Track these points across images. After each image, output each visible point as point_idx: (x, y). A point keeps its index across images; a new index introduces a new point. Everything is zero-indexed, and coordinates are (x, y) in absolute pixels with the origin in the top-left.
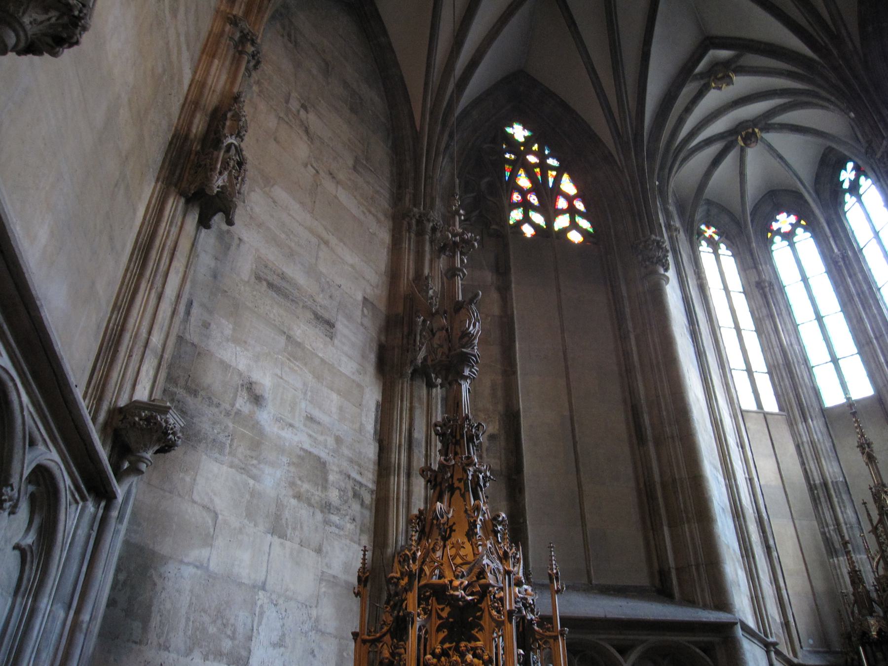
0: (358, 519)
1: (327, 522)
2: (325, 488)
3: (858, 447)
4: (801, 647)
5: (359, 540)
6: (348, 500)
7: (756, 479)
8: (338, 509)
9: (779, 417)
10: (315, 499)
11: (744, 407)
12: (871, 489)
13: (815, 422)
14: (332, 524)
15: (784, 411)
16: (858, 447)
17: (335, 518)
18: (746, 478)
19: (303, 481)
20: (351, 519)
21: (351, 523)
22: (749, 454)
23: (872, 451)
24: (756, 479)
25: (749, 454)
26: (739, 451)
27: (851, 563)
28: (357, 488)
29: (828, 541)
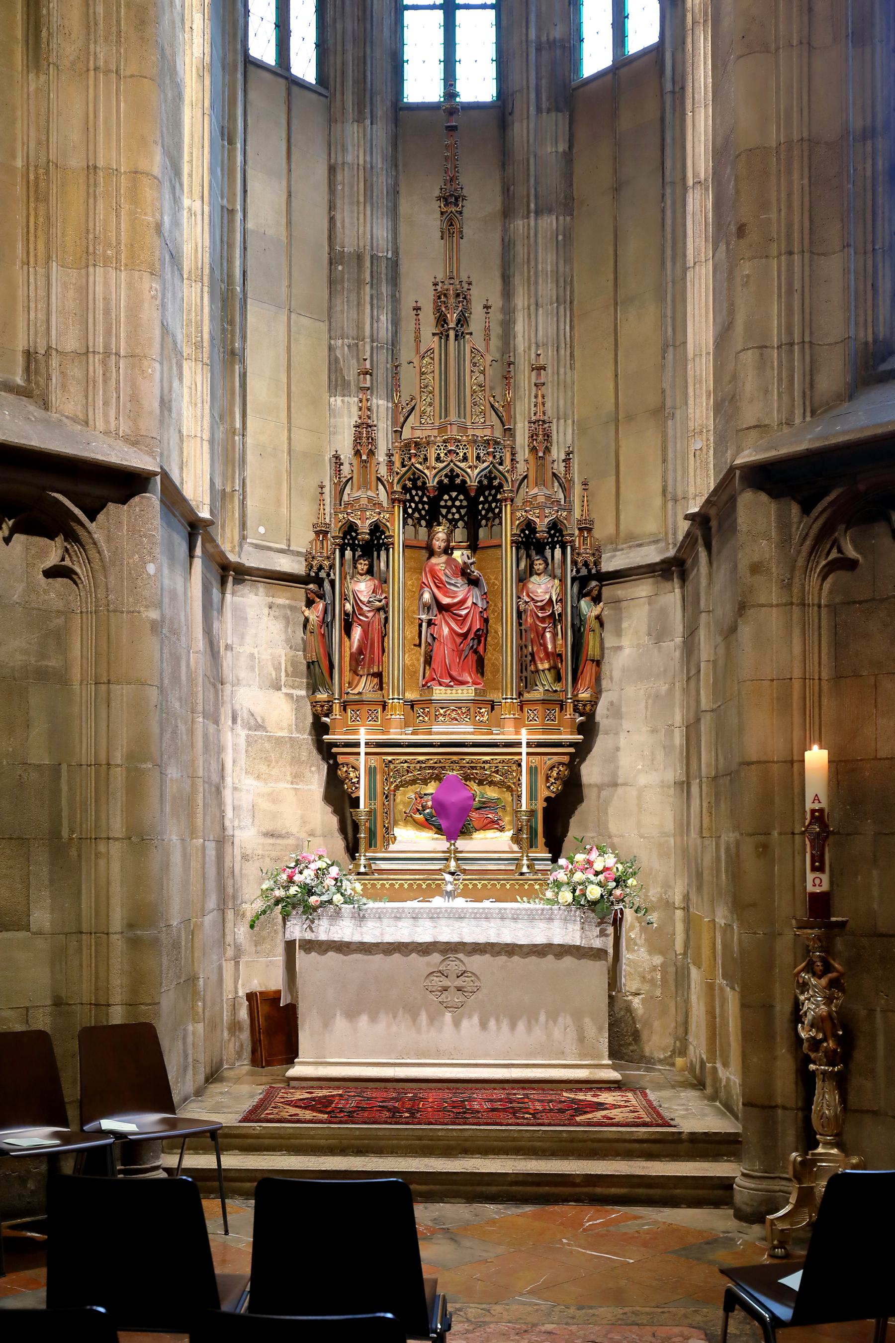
3: (439, 199)
7: (239, 216)
9: (314, 97)
11: (255, 51)
12: (435, 284)
13: (374, 126)
15: (327, 88)
16: (439, 199)
18: (222, 207)
22: (239, 158)
23: (461, 213)
24: (239, 216)
25: (239, 158)
26: (223, 146)
27: (366, 410)
29: (334, 366)
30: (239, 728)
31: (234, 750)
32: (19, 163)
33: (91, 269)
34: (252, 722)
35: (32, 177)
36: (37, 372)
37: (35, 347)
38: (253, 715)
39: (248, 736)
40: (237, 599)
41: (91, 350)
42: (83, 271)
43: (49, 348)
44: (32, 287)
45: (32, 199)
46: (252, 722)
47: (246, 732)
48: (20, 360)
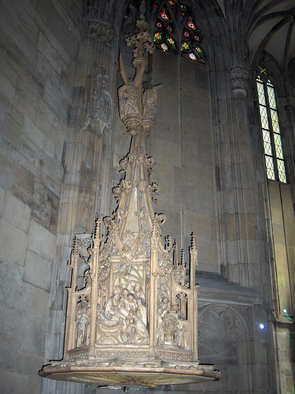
0: (49, 214)
1: (33, 214)
2: (33, 193)
4: (280, 314)
5: (50, 228)
6: (45, 202)
8: (39, 207)
10: (26, 199)
14: (35, 216)
17: (37, 213)
19: (19, 186)
20: (45, 214)
21: (46, 217)
28: (50, 195)
30: (284, 375)
31: (283, 383)
32: (216, 215)
33: (239, 241)
34: (288, 373)
35: (220, 218)
36: (224, 270)
37: (223, 264)
38: (287, 371)
39: (286, 378)
40: (279, 333)
41: (240, 263)
42: (236, 241)
43: (228, 264)
44: (222, 247)
45: (220, 224)
46: (288, 373)
47: (286, 377)
48: (219, 267)
